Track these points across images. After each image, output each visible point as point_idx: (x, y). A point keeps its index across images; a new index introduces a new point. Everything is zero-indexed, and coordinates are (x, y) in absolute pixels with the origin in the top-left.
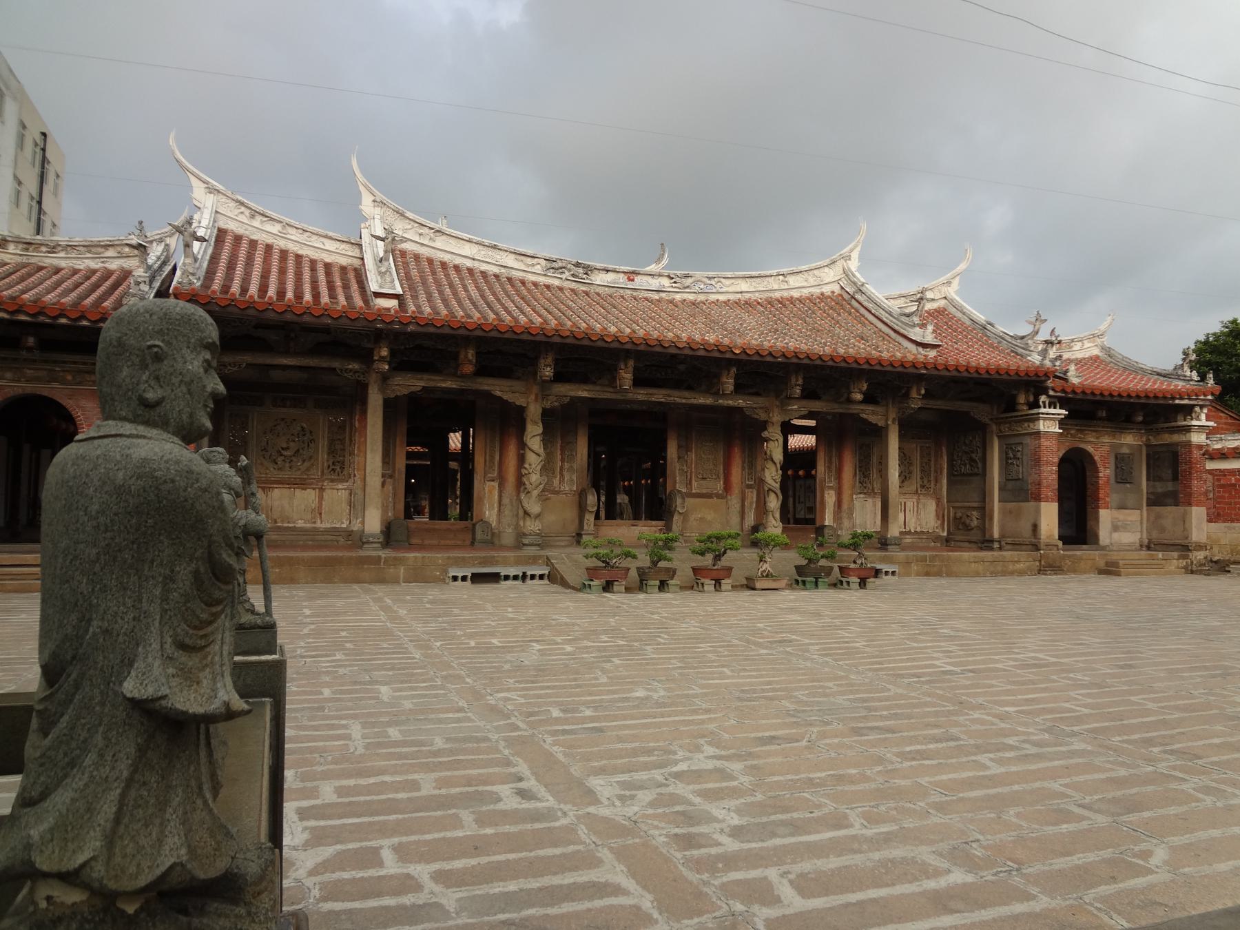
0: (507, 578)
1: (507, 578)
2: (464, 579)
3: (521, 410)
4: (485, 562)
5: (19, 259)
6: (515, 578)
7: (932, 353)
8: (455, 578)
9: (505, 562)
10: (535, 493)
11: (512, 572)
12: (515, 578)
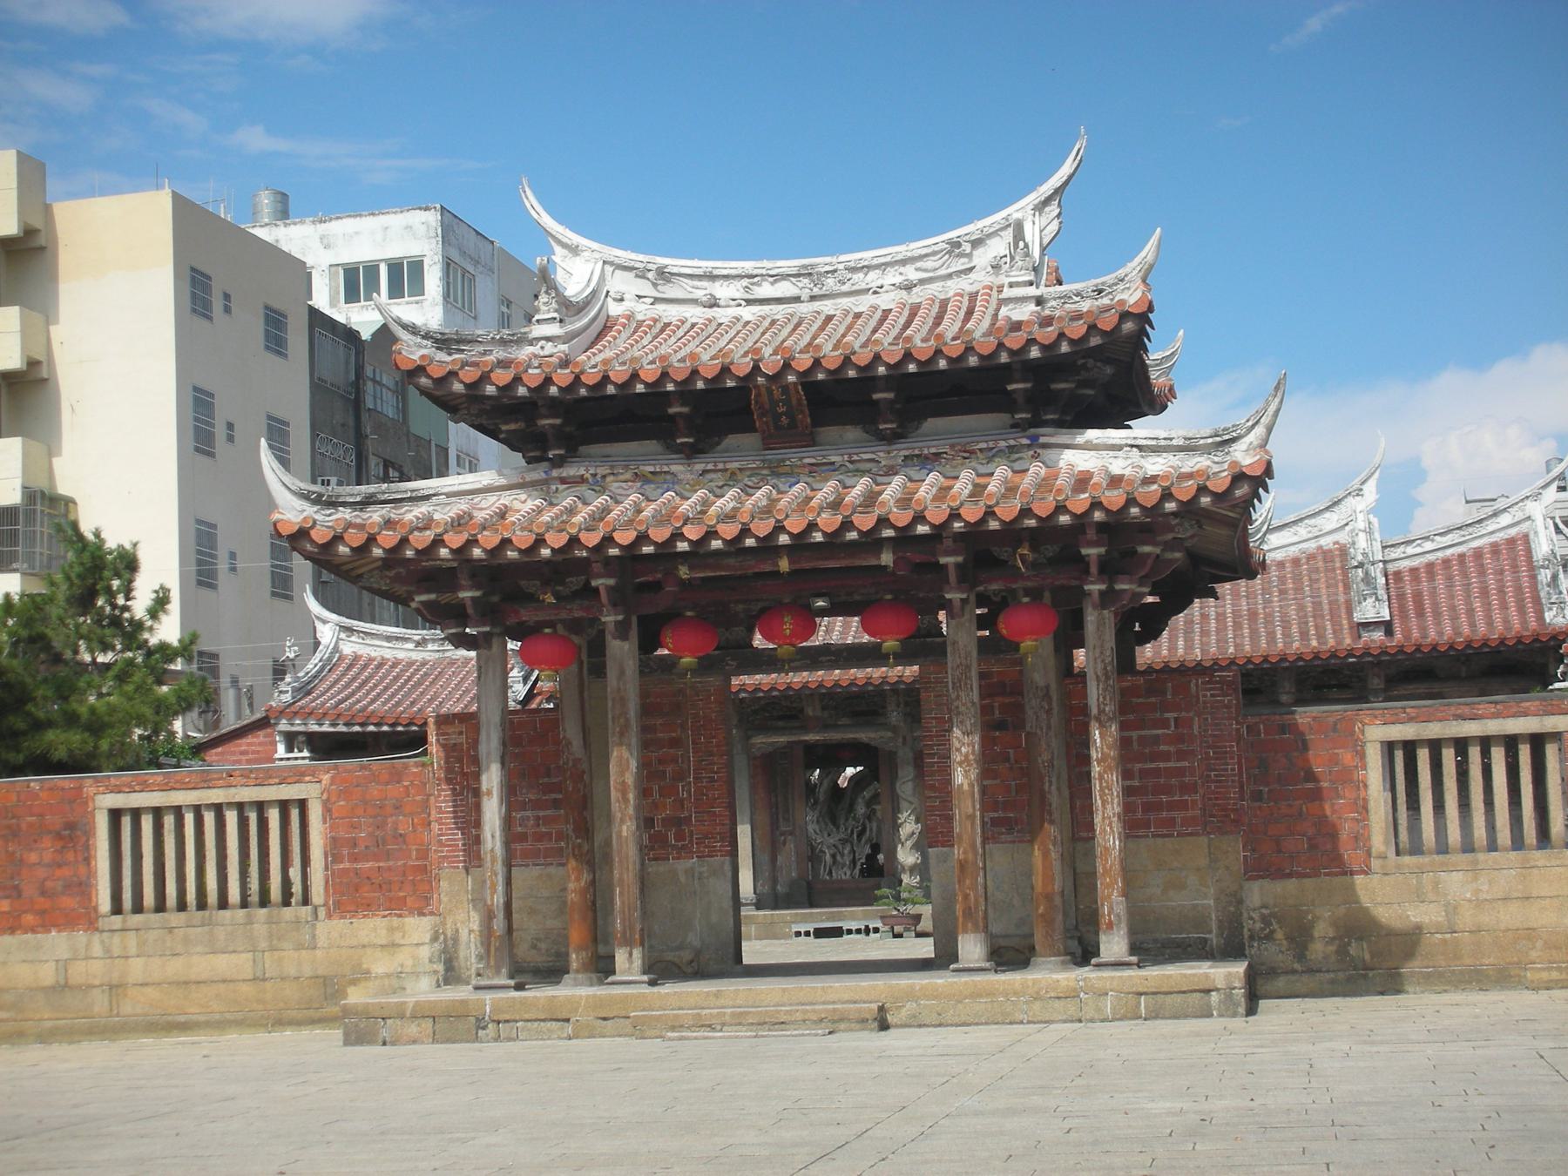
0: (849, 932)
1: (849, 932)
2: (807, 934)
3: (892, 755)
4: (832, 917)
5: (437, 655)
6: (858, 931)
7: (1378, 635)
8: (798, 934)
9: (853, 917)
10: (909, 844)
11: (854, 926)
12: (858, 931)
